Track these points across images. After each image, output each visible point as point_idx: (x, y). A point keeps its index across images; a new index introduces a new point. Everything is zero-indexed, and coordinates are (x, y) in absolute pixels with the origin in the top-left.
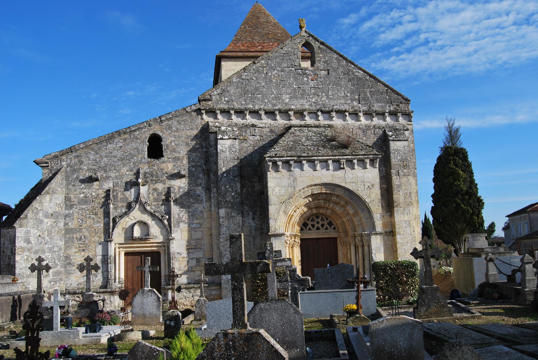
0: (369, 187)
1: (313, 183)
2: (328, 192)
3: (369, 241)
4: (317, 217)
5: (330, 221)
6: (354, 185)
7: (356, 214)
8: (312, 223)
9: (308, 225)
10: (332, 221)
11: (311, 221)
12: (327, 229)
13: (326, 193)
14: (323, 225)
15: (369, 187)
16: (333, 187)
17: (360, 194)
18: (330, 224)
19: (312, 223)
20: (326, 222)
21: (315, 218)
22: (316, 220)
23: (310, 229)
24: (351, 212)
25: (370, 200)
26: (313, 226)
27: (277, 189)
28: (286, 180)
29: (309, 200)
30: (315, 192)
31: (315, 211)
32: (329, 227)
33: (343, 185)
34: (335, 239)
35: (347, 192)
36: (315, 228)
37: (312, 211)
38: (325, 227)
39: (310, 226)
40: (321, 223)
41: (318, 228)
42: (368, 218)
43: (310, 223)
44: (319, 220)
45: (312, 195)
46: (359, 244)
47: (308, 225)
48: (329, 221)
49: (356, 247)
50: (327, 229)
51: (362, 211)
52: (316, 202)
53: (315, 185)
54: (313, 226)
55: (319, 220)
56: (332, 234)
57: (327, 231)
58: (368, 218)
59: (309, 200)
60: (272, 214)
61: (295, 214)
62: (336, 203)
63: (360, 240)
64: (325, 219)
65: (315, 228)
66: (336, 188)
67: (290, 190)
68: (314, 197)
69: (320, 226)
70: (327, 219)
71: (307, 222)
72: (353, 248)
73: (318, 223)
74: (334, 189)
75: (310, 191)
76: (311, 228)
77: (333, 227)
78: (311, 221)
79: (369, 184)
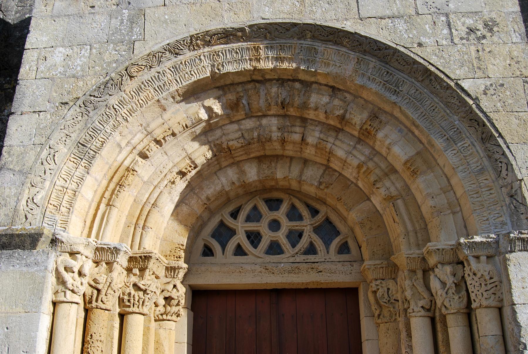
0: (471, 30)
1: (215, 26)
2: (285, 65)
3: (501, 284)
4: (274, 204)
5: (328, 221)
6: (401, 25)
7: (423, 160)
8: (252, 226)
9: (233, 232)
10: (334, 218)
11: (248, 219)
12: (311, 250)
13: (283, 80)
14: (295, 237)
15: (471, 30)
16: (307, 43)
17: (433, 59)
18: (327, 230)
19: (252, 226)
20: (307, 225)
21: (263, 208)
22: (268, 215)
23: (239, 251)
24: (400, 153)
25: (482, 84)
26: (254, 238)
27: (58, 56)
28: (102, 19)
29: (209, 110)
30: (230, 68)
31: (252, 173)
32: (319, 244)
33: (349, 26)
34: (350, 294)
35: (373, 62)
36: (264, 244)
37: (243, 172)
38: (304, 243)
39: (241, 238)
40: (286, 225)
41: (275, 249)
42: (482, 171)
43: (241, 226)
44: (281, 214)
45: (216, 84)
46: (450, 304)
47: (233, 232)
48: (320, 218)
49: (436, 323)
50: (311, 250)
51: (450, 141)
52: (249, 124)
53: (227, 35)
54: (254, 238)
55: (281, 214)
56: (330, 271)
57: (311, 258)
58: (482, 171)
59: (209, 110)
60: (17, 150)
61: (145, 170)
62: (339, 127)
63: (450, 281)
64: (305, 213)
65: (264, 244)
66: (320, 47)
67: (111, 54)
68: (231, 97)
69: (281, 236)
70: (315, 212)
71: (230, 222)
72: (420, 327)
73: (275, 225)
74: (312, 50)
75: (206, 63)
76: (247, 245)
77: (336, 243)
78: (248, 219)
79: (469, 22)
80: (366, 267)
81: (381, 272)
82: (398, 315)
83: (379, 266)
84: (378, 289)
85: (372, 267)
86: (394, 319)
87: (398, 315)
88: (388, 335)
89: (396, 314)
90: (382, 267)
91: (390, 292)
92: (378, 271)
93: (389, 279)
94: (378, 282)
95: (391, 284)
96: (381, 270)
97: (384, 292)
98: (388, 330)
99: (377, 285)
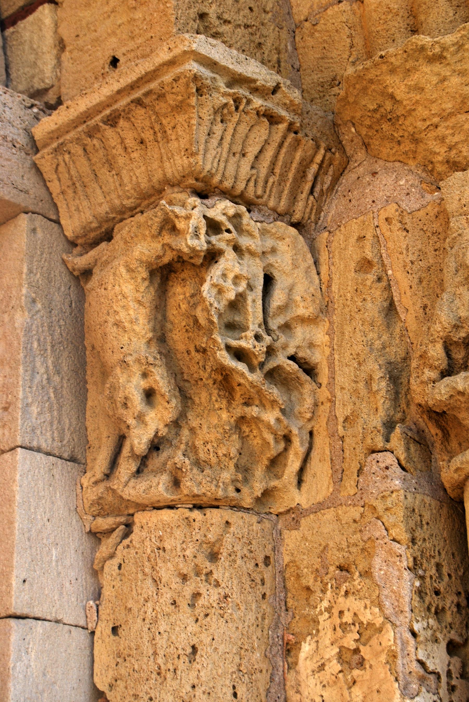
80: (194, 67)
81: (252, 151)
82: (293, 464)
83: (258, 102)
84: (213, 256)
85: (221, 84)
86: (258, 488)
87: (293, 464)
88: (210, 596)
89: (275, 463)
90: (273, 119)
91: (278, 297)
92: (243, 129)
93: (280, 216)
94: (221, 209)
95: (287, 250)
96: (262, 132)
97: (250, 287)
98: (214, 557)
99: (214, 227)
